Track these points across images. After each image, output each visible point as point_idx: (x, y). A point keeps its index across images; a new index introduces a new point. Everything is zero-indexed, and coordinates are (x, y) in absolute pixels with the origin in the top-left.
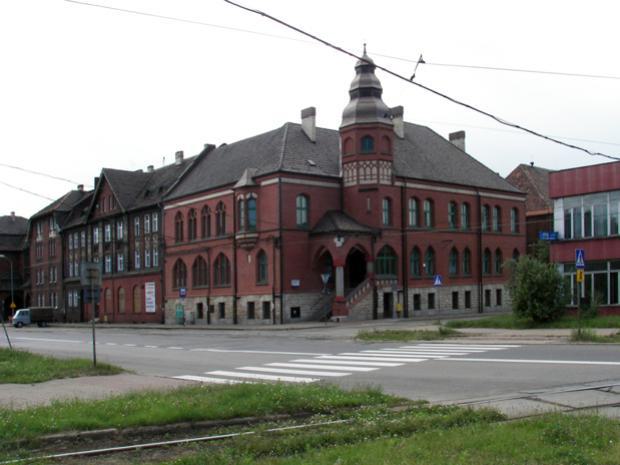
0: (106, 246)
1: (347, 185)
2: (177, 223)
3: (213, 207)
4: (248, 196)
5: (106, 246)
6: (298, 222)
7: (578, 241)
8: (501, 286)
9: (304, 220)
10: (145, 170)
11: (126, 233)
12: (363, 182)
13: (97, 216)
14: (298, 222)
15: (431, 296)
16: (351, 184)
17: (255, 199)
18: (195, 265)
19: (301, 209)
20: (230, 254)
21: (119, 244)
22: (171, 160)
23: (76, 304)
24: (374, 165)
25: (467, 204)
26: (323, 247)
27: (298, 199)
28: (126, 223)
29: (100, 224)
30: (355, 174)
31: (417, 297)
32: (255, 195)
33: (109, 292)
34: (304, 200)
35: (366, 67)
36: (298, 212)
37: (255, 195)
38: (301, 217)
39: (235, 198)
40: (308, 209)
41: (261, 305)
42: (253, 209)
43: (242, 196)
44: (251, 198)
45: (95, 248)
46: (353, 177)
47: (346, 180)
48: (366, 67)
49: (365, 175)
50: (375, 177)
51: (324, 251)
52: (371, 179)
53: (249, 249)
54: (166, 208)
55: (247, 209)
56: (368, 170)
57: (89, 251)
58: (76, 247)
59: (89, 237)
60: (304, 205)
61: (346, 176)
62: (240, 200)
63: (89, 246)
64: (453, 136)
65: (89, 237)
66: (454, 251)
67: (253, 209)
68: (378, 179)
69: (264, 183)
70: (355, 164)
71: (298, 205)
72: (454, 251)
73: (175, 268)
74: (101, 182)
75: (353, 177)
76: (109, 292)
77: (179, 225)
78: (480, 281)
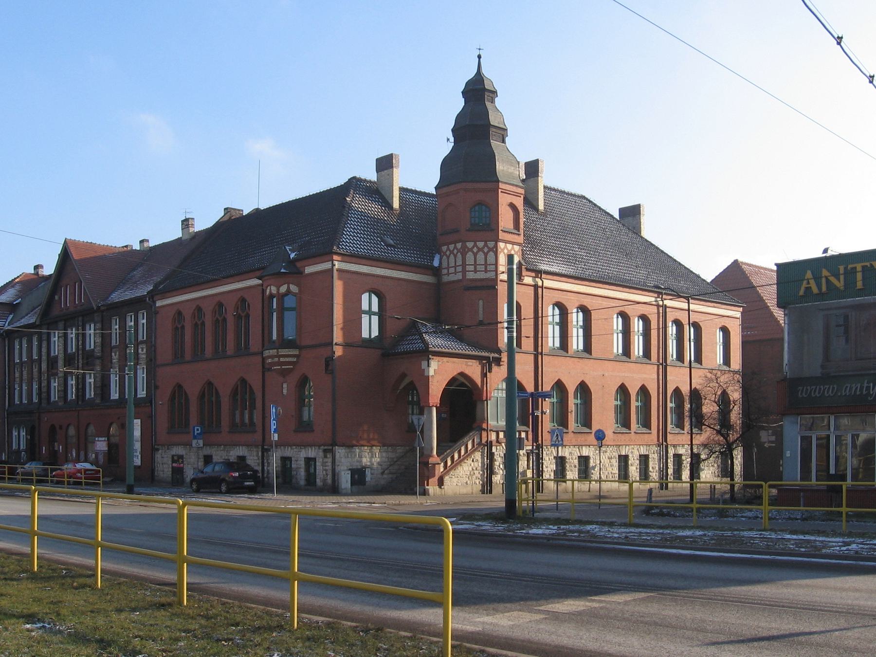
0: (69, 360)
1: (445, 279)
2: (176, 328)
3: (208, 309)
4: (283, 289)
5: (69, 360)
6: (365, 334)
7: (91, 404)
8: (311, 453)
9: (375, 333)
10: (137, 247)
11: (99, 340)
12: (471, 275)
13: (55, 312)
14: (365, 334)
15: (584, 461)
16: (453, 278)
17: (295, 294)
18: (202, 396)
19: (370, 313)
20: (255, 381)
21: (88, 359)
22: (174, 233)
23: (23, 446)
24: (479, 250)
25: (644, 318)
26: (403, 376)
27: (365, 297)
28: (99, 325)
29: (61, 325)
30: (459, 262)
31: (561, 462)
32: (294, 288)
33: (72, 431)
34: (375, 299)
35: (477, 92)
36: (365, 319)
37: (294, 288)
38: (370, 328)
39: (263, 292)
40: (382, 314)
41: (302, 463)
42: (292, 309)
43: (274, 290)
44: (288, 292)
45: (52, 362)
46: (455, 267)
47: (445, 271)
48: (477, 92)
49: (475, 265)
50: (459, 269)
51: (406, 381)
52: (486, 271)
53: (284, 373)
54: (159, 304)
55: (282, 310)
56: (481, 256)
57: (44, 366)
58: (25, 359)
59: (44, 344)
60: (375, 308)
61: (445, 265)
62: (272, 296)
63: (80, 352)
64: (623, 212)
65: (44, 344)
66: (623, 390)
67: (292, 309)
68: (464, 272)
69: (309, 270)
70: (459, 245)
71: (365, 306)
72: (623, 390)
73: (172, 398)
74: (65, 256)
75: (455, 267)
76: (72, 431)
77: (178, 331)
78: (329, 451)
